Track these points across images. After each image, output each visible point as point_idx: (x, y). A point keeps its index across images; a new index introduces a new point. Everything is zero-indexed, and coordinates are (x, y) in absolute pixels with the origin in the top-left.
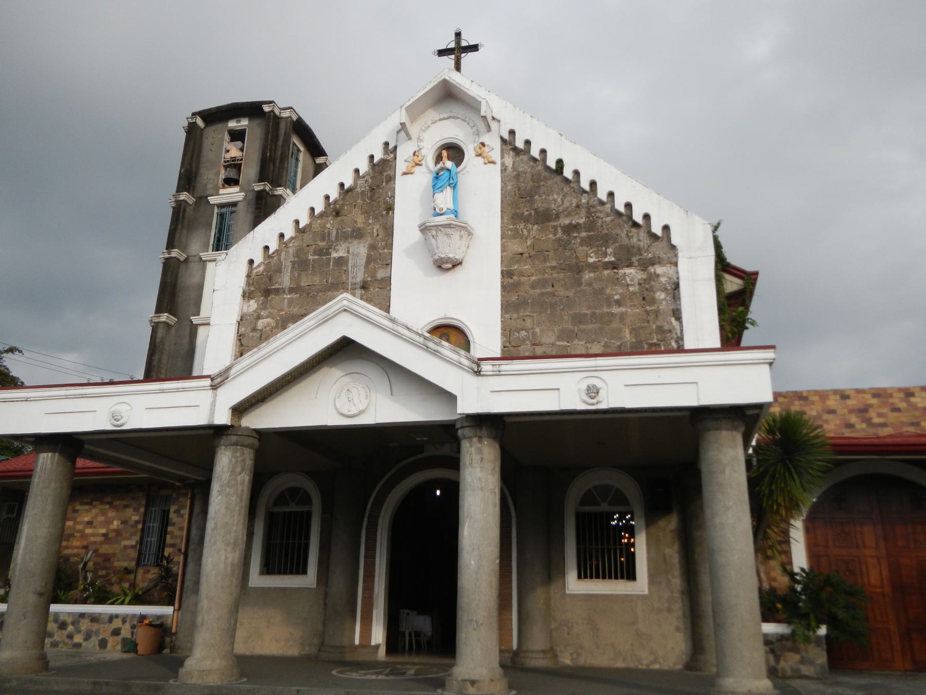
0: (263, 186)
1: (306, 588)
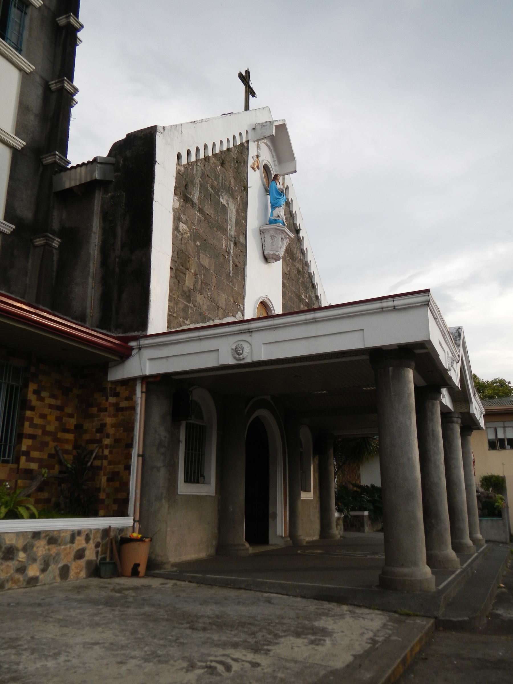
0: (80, 27)
1: (210, 496)
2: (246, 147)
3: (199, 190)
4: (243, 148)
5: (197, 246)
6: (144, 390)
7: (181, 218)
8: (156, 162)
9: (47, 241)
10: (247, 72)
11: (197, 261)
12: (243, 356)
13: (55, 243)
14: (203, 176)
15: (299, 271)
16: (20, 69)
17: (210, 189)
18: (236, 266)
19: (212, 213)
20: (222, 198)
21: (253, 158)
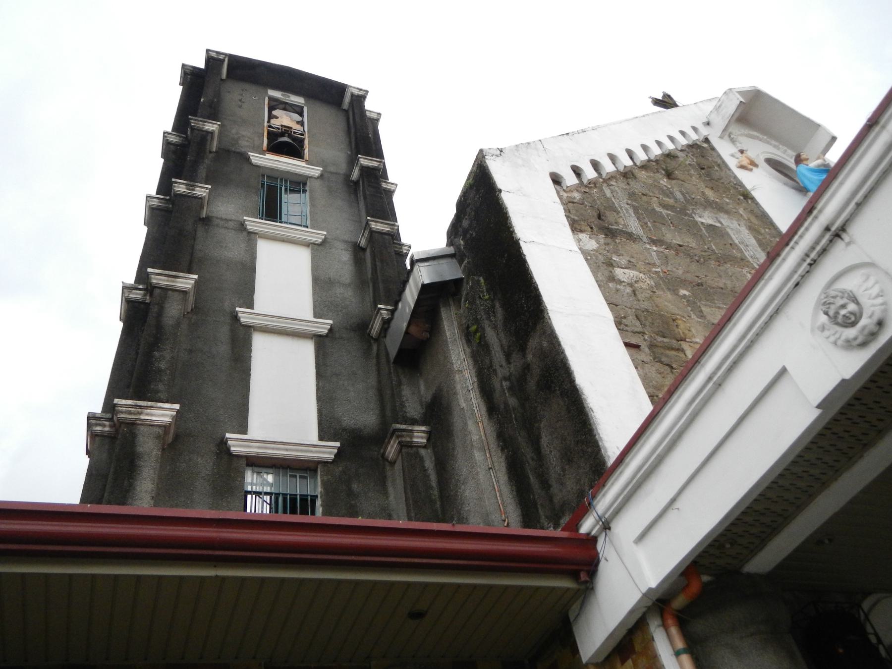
0: (378, 163)
2: (709, 148)
3: (633, 215)
5: (684, 296)
6: (680, 644)
7: (613, 262)
8: (500, 191)
9: (400, 440)
11: (700, 321)
12: (870, 317)
13: (418, 437)
14: (632, 195)
16: (307, 244)
17: (662, 210)
19: (688, 242)
20: (700, 217)
21: (733, 156)
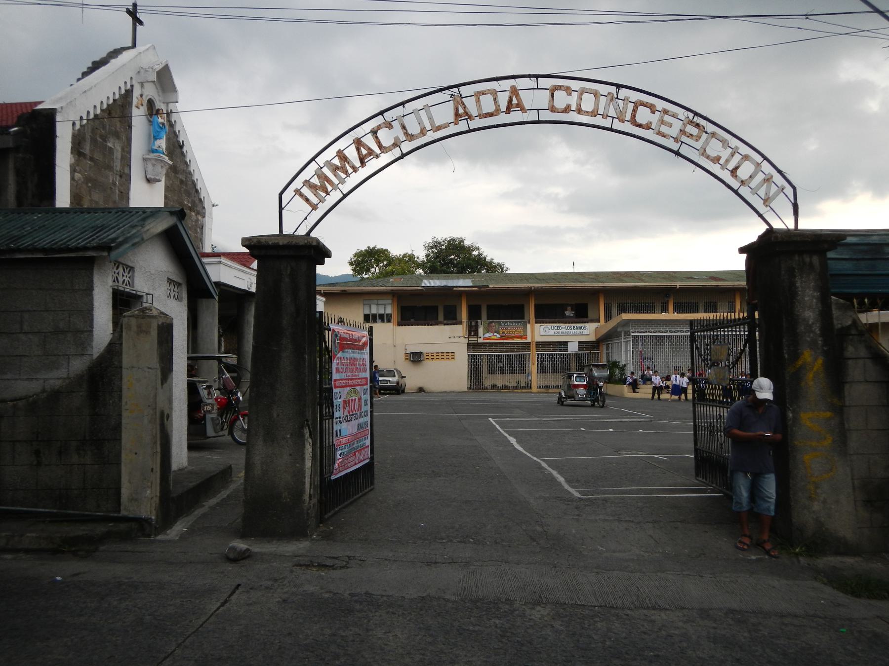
4: (129, 93)
5: (89, 187)
8: (57, 136)
10: (135, 5)
15: (182, 182)
18: (121, 192)
21: (137, 98)
